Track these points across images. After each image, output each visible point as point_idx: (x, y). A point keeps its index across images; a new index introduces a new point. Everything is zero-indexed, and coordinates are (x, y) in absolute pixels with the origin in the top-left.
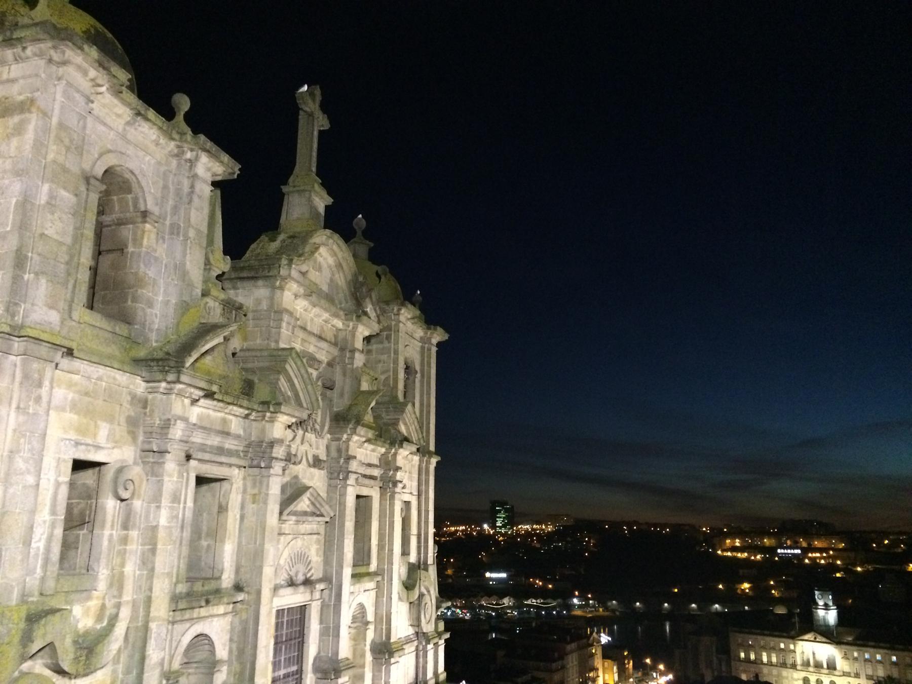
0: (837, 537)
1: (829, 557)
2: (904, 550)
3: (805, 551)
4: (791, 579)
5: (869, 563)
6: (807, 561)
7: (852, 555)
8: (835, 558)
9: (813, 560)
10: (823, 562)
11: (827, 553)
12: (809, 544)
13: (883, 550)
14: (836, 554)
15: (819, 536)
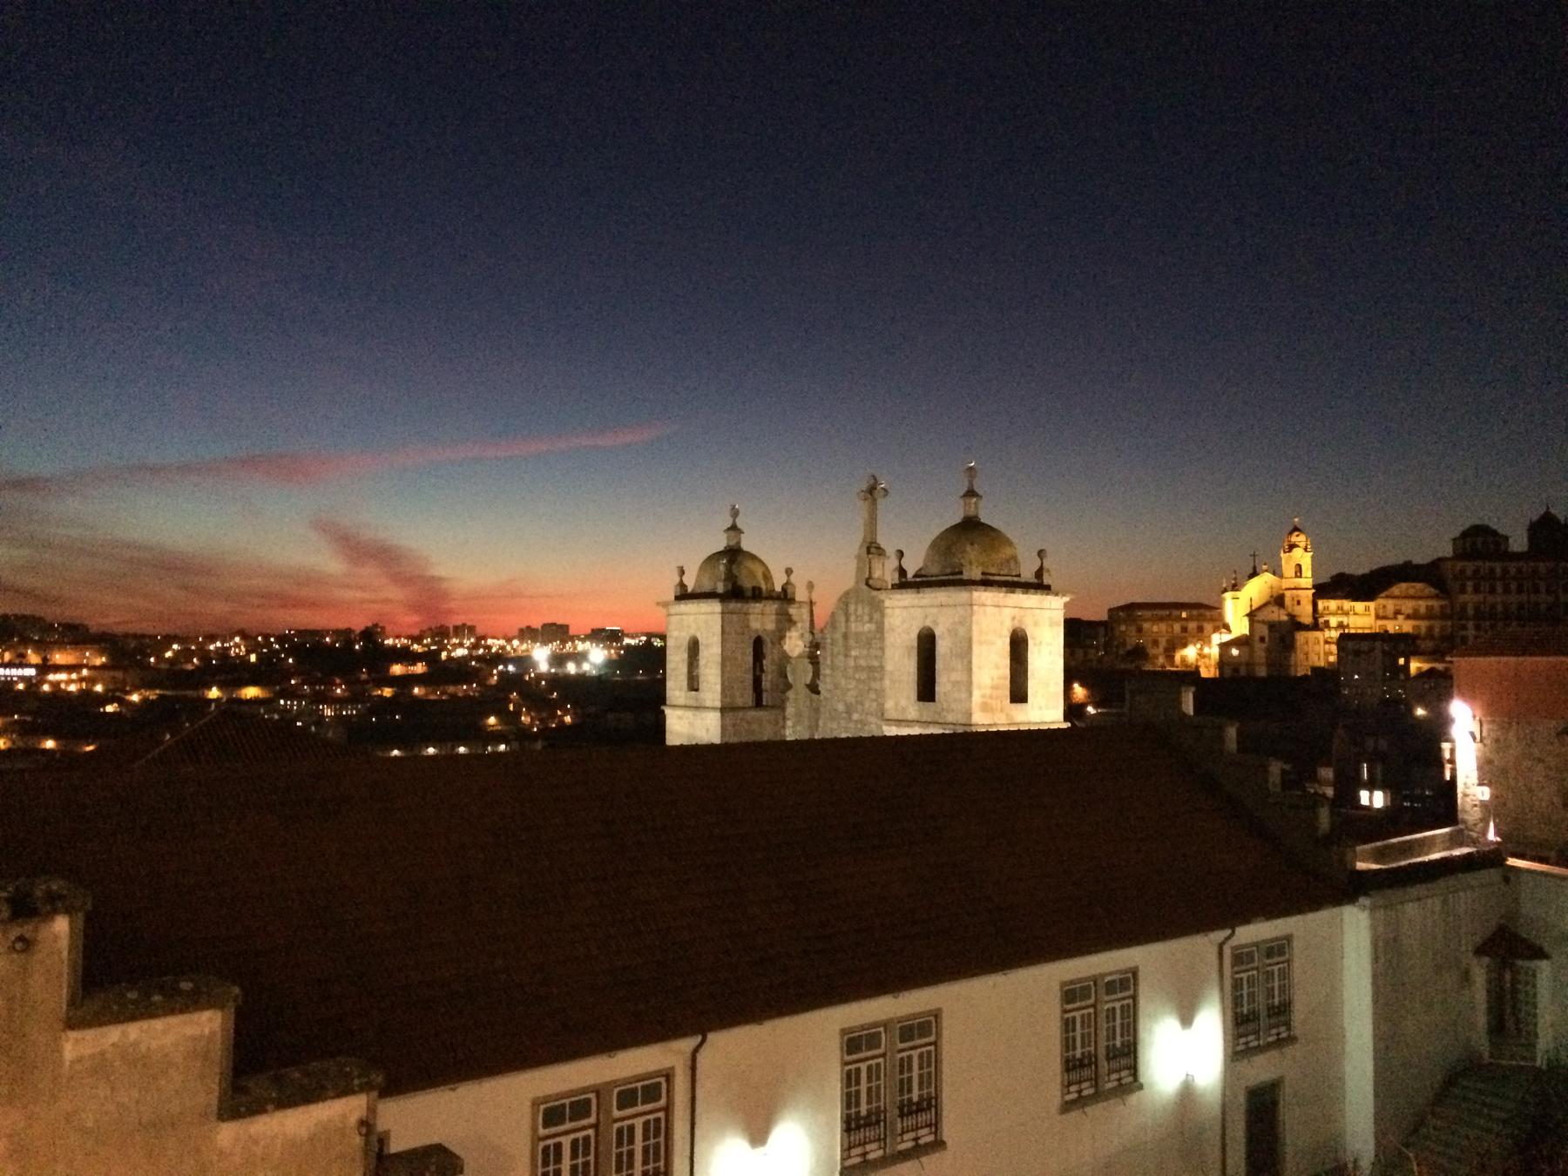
0: (95, 646)
1: (81, 680)
2: (197, 667)
3: (45, 668)
4: (29, 719)
5: (150, 685)
6: (46, 688)
7: (119, 674)
8: (91, 681)
9: (55, 685)
10: (73, 688)
11: (79, 673)
12: (45, 659)
13: (163, 666)
14: (93, 673)
15: (61, 645)
